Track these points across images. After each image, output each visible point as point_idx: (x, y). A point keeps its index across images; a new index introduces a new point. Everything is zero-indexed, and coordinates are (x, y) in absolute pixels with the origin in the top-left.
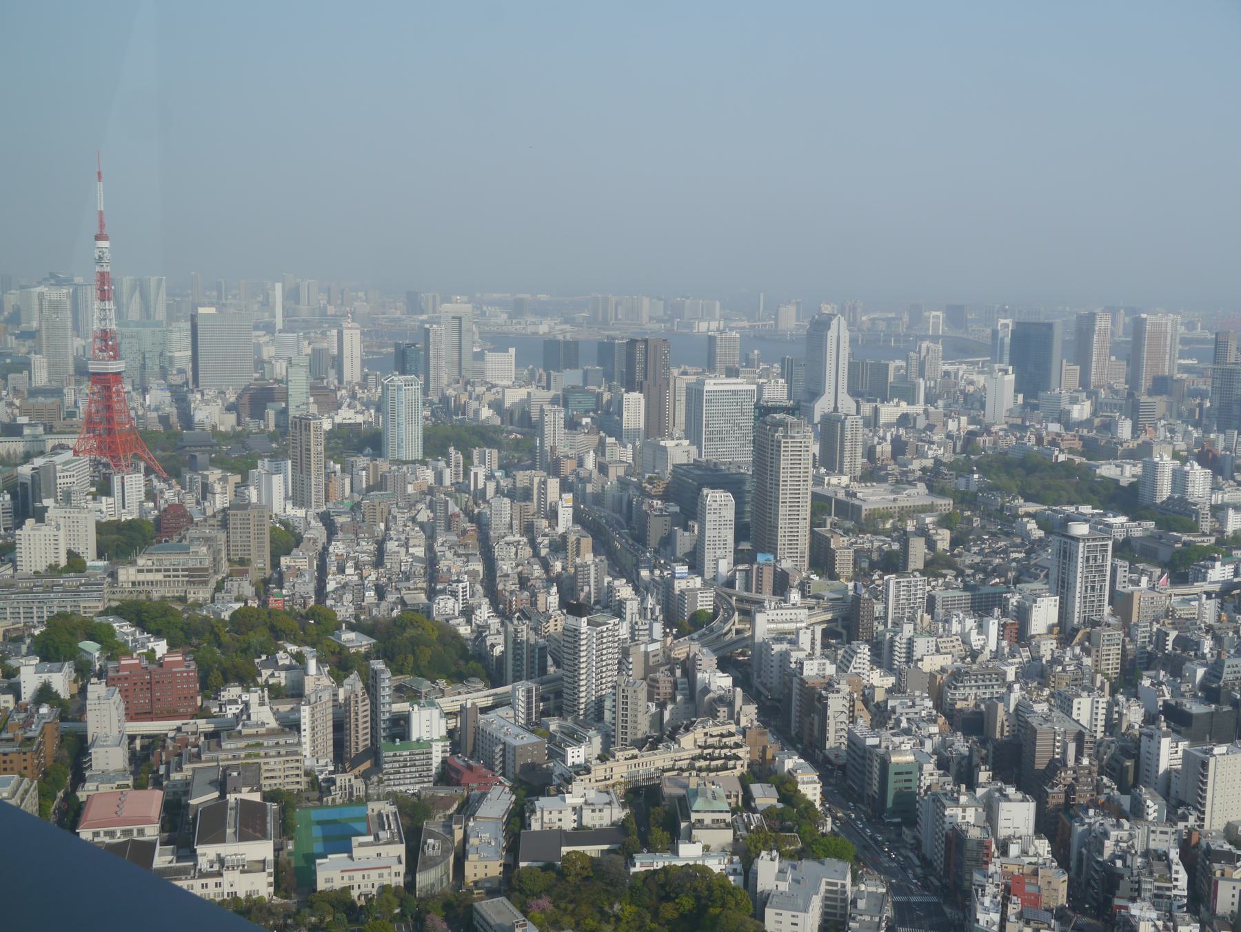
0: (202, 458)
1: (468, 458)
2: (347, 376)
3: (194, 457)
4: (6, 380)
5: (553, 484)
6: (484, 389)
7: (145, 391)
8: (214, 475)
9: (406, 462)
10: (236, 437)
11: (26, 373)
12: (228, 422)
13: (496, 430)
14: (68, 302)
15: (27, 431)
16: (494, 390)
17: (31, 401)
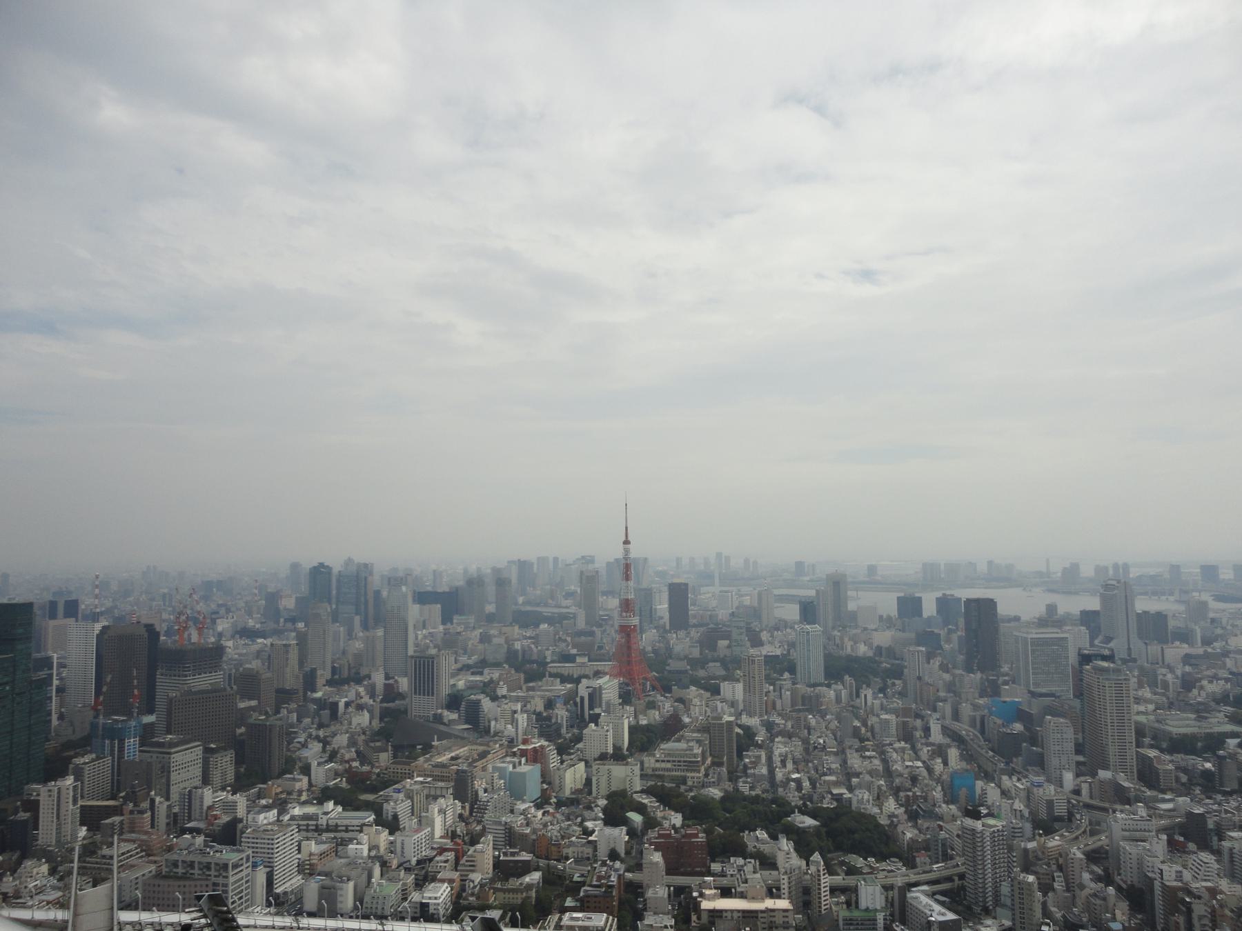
6: (859, 631)
7: (642, 632)
9: (814, 685)
10: (701, 663)
13: (870, 659)
15: (579, 660)
17: (577, 639)
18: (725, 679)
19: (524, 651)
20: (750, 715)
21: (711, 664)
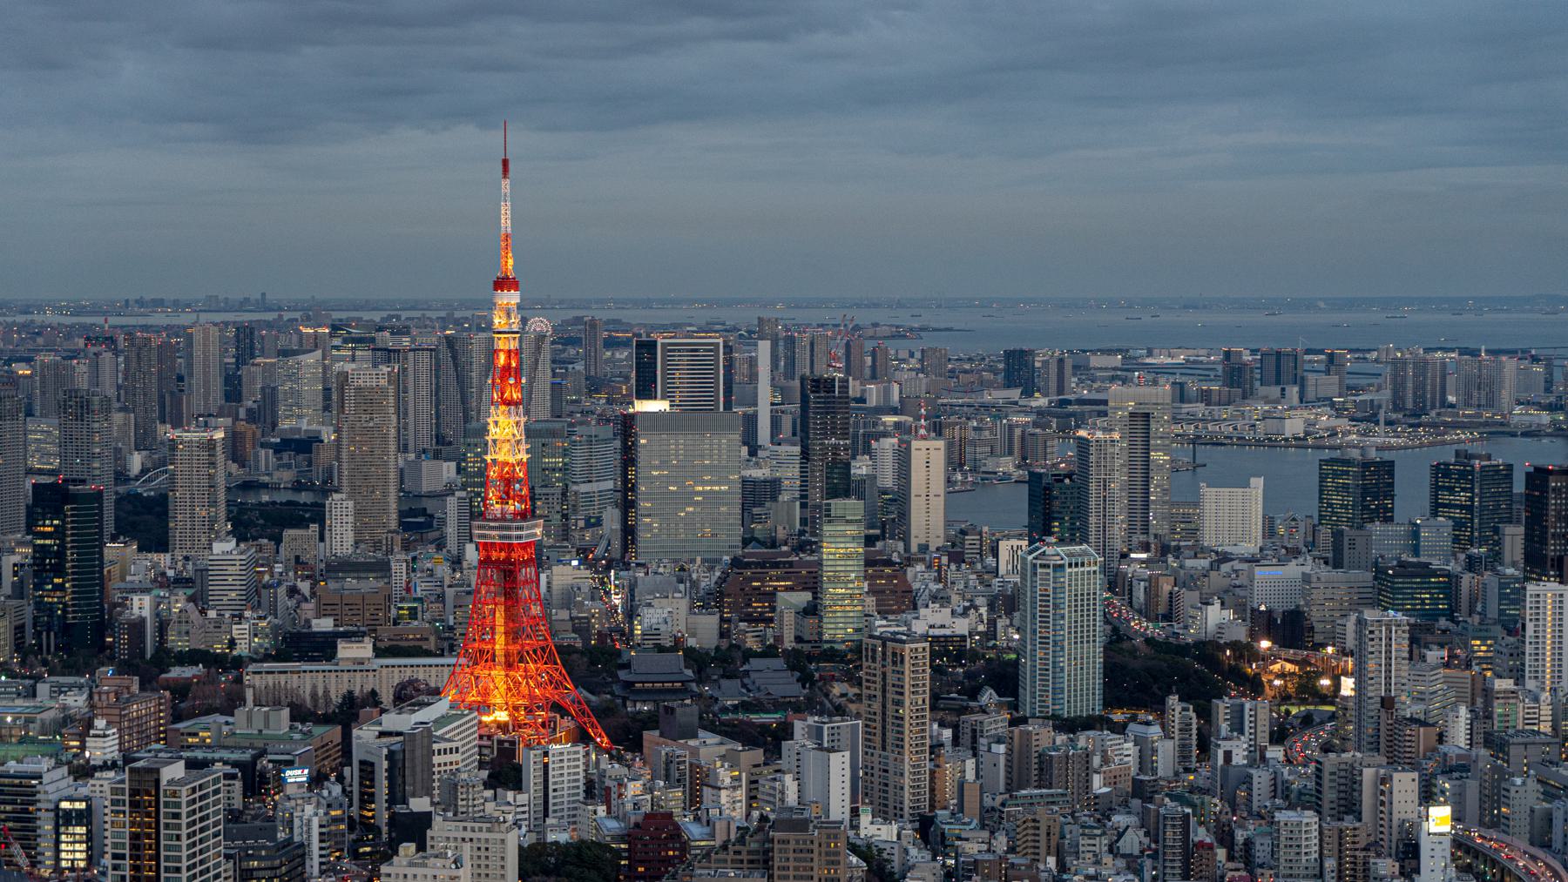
0: (687, 710)
1: (1205, 714)
2: (917, 536)
3: (673, 710)
4: (278, 540)
5: (1405, 784)
6: (1204, 563)
8: (709, 747)
11: (314, 527)
12: (705, 631)
14: (391, 391)
15: (346, 651)
16: (1225, 568)
18: (799, 709)
19: (162, 627)
20: (885, 813)
21: (755, 663)
